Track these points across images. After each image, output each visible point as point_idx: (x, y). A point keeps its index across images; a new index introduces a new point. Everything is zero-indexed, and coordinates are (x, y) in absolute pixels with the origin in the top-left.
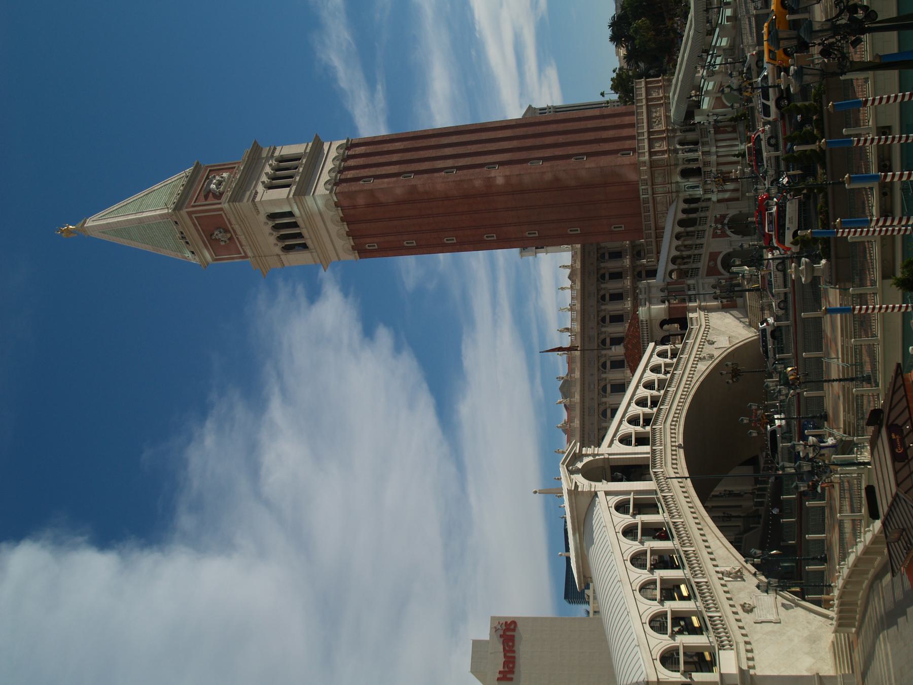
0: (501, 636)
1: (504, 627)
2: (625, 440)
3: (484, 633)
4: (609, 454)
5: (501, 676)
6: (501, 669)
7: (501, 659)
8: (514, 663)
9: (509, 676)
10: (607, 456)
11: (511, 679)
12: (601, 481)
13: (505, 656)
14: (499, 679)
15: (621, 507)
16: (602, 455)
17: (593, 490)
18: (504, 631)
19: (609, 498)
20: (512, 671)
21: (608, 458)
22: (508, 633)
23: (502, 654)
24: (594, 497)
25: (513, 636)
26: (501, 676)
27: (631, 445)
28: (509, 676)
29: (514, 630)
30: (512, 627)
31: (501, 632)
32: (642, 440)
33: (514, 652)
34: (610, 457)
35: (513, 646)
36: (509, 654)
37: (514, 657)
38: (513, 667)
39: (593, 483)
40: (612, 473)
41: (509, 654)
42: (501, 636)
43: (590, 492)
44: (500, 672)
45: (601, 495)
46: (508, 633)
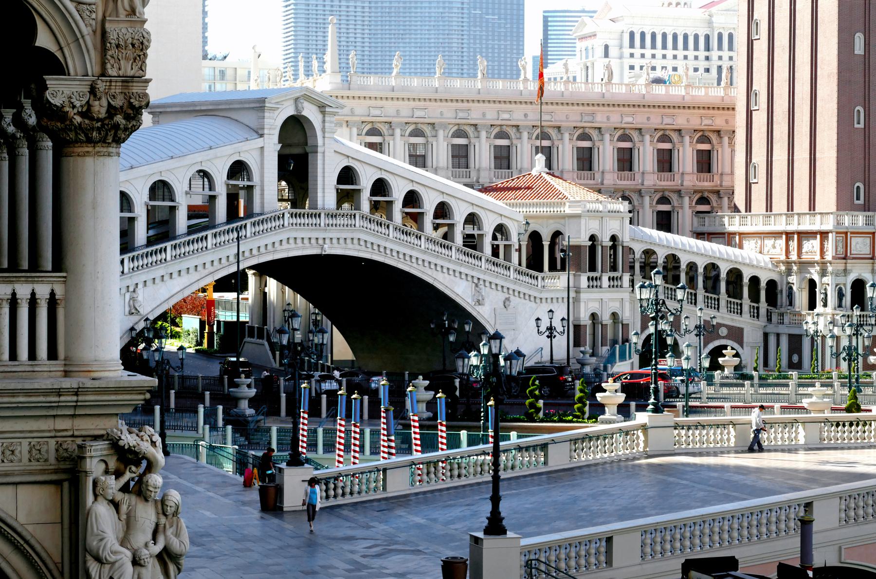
2: (347, 175)
4: (324, 153)
10: (320, 149)
12: (279, 143)
15: (238, 169)
16: (324, 144)
17: (266, 131)
19: (256, 154)
21: (317, 152)
24: (257, 132)
27: (338, 184)
32: (344, 197)
34: (320, 156)
39: (277, 132)
40: (294, 157)
43: (263, 129)
45: (259, 142)
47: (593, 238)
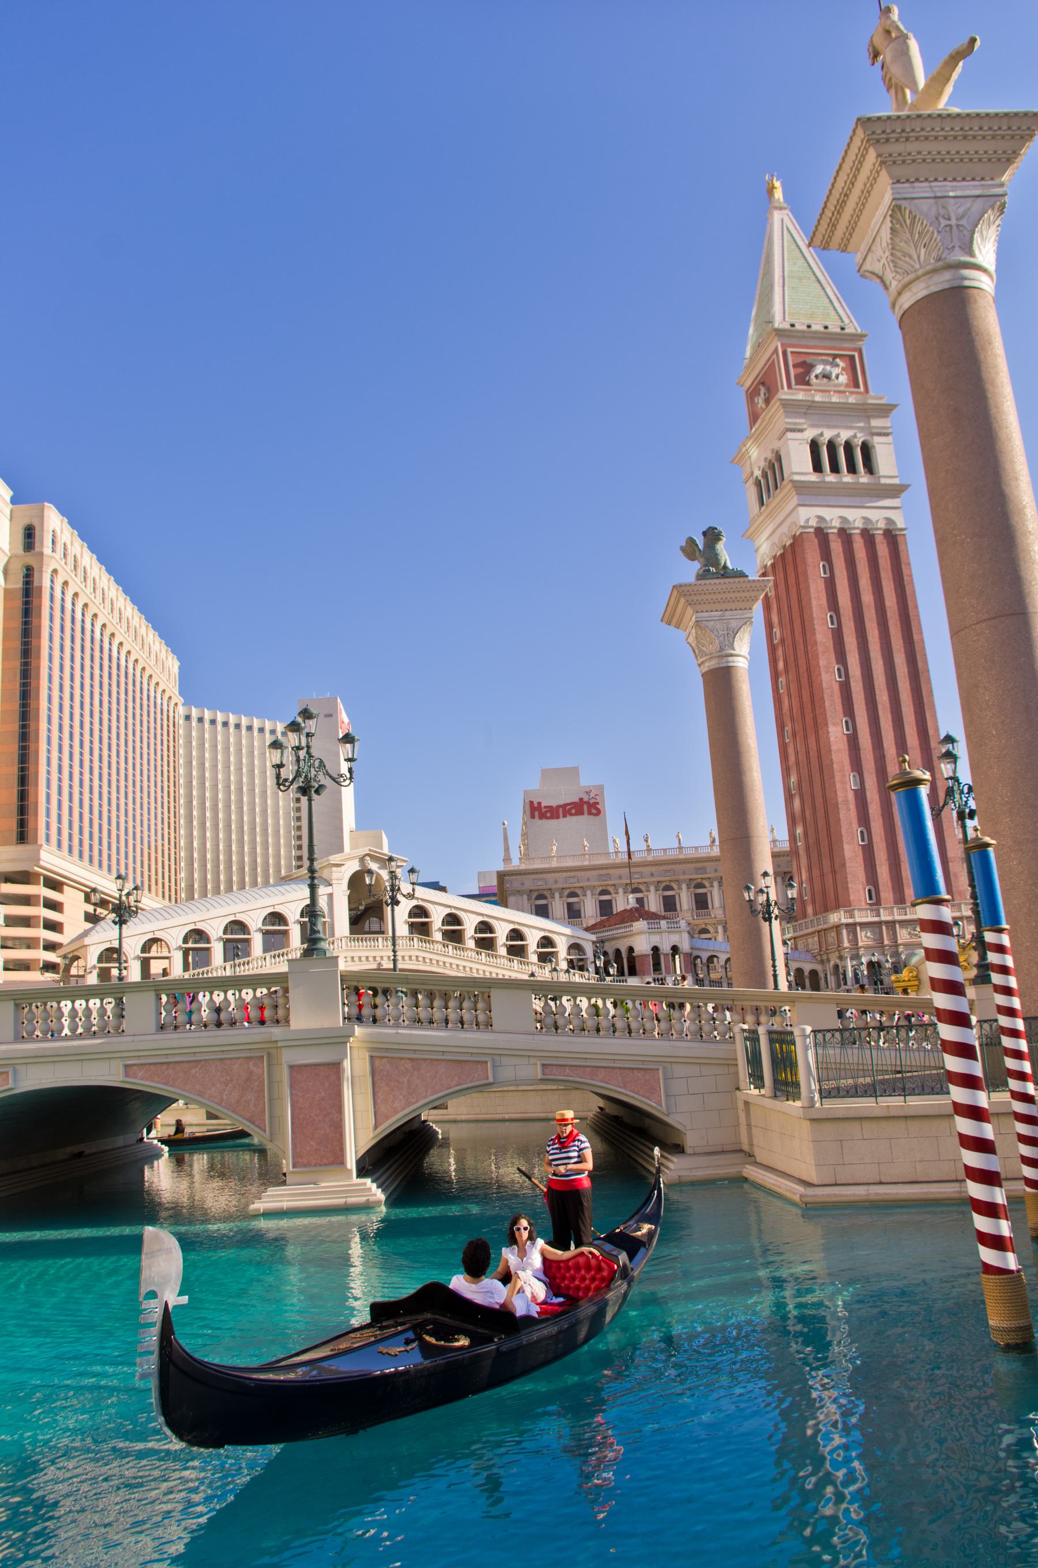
0: (581, 799)
1: (592, 801)
3: (587, 780)
5: (536, 805)
6: (543, 805)
7: (554, 803)
8: (552, 817)
9: (536, 813)
11: (533, 817)
13: (559, 807)
14: (531, 803)
18: (588, 803)
20: (542, 816)
22: (585, 807)
23: (562, 803)
25: (582, 813)
26: (536, 805)
28: (536, 813)
29: (590, 813)
30: (594, 811)
31: (586, 799)
33: (564, 816)
35: (572, 815)
36: (561, 810)
37: (558, 817)
38: (547, 818)
41: (561, 810)
42: (581, 799)
44: (539, 804)
46: (585, 807)
47: (655, 949)
